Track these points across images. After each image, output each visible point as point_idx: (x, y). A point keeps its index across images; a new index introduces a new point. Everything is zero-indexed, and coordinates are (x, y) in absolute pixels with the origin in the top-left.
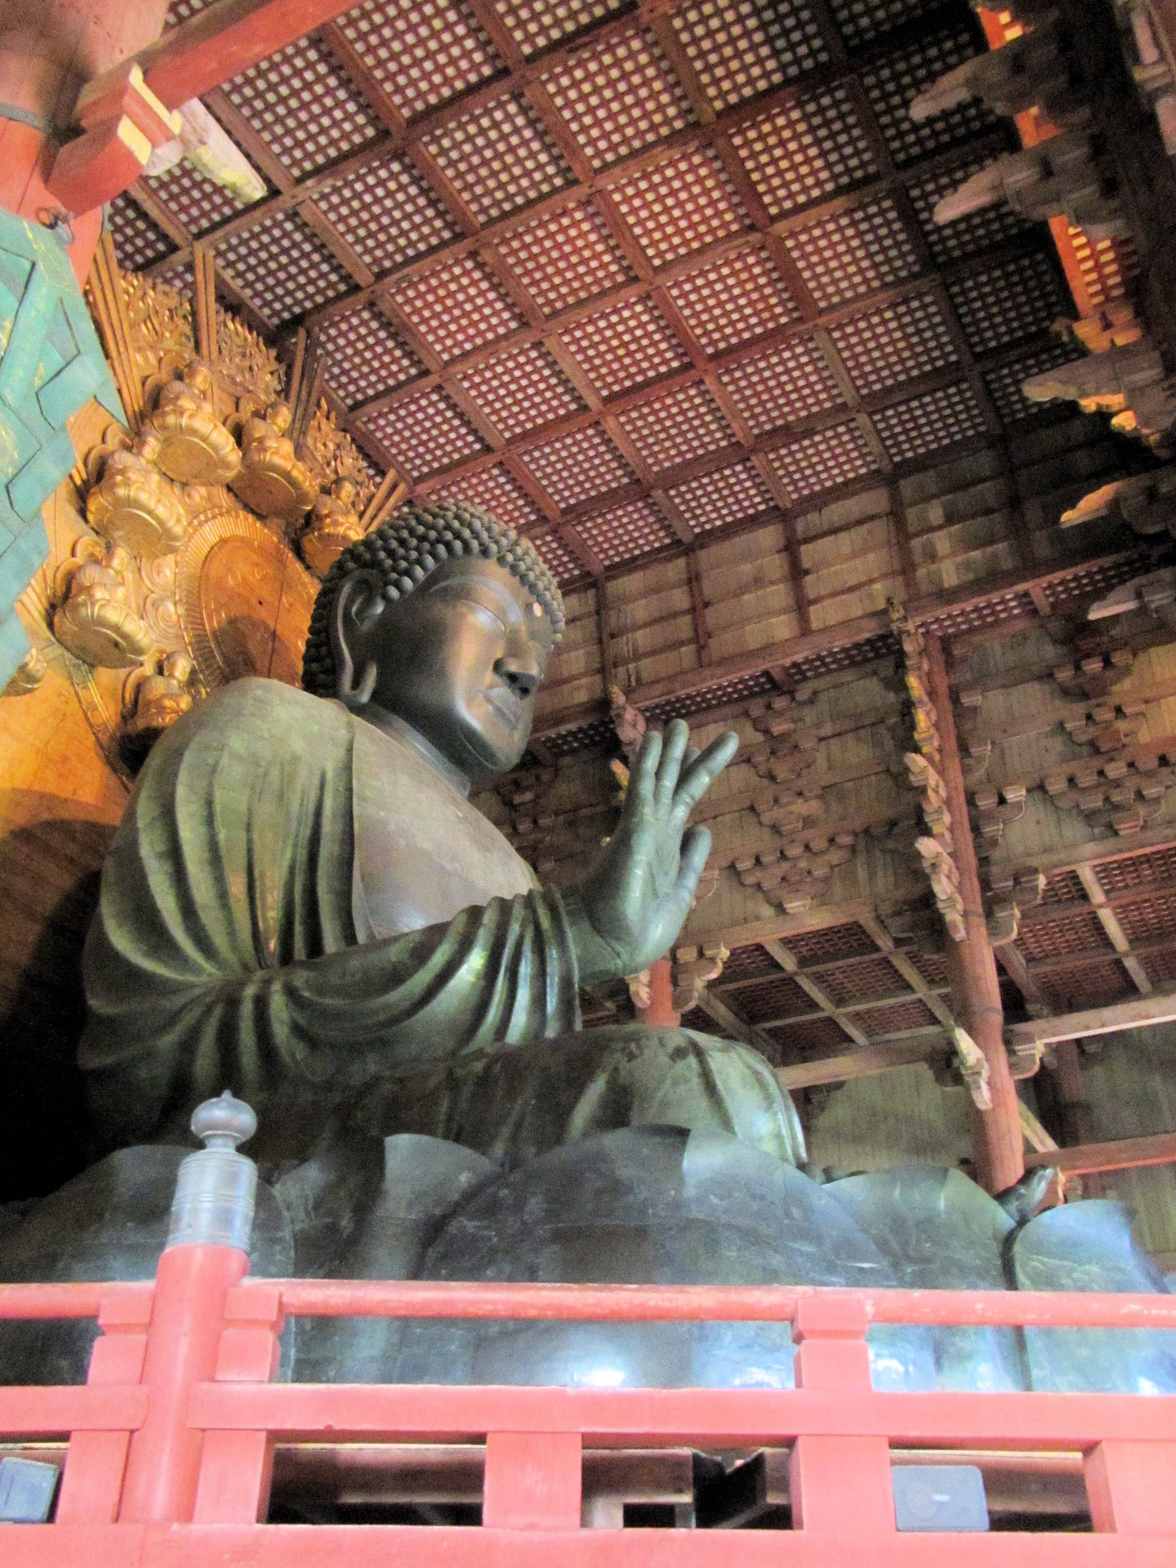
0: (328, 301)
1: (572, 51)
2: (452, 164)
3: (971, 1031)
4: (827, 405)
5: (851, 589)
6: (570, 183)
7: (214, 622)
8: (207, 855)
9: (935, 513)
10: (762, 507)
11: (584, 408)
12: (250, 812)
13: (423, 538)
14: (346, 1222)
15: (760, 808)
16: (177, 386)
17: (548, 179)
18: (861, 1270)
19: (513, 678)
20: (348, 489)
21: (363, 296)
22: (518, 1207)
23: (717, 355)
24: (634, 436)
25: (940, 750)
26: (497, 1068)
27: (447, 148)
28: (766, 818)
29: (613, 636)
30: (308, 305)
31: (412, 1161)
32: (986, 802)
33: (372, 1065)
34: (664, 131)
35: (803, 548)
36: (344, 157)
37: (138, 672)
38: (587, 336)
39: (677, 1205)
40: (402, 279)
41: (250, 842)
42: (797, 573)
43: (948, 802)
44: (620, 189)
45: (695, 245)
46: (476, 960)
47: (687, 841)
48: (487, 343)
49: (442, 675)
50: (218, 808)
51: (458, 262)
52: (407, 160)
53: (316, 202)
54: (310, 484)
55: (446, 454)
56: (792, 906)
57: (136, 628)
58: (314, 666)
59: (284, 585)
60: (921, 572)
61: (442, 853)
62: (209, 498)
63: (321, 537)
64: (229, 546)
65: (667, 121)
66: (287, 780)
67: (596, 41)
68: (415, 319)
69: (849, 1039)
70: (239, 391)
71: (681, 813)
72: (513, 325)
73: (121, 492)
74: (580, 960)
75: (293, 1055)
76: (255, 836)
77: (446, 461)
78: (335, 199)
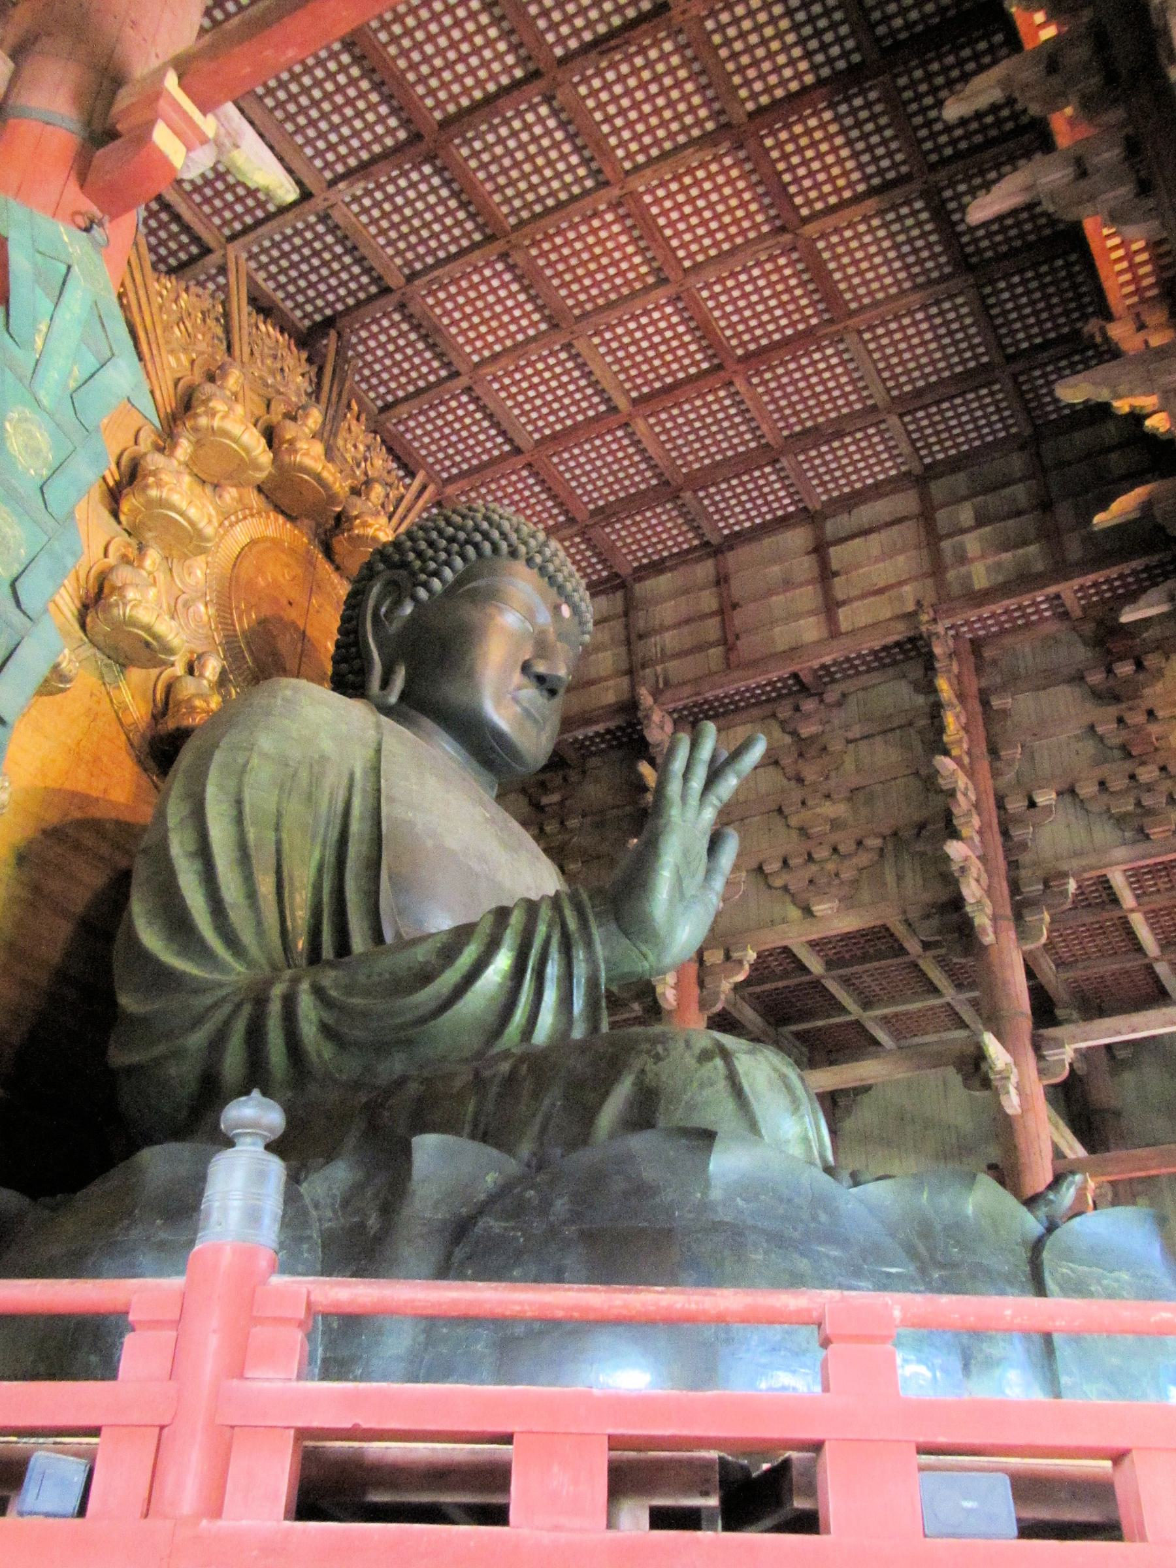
0: (359, 304)
1: (602, 53)
2: (484, 166)
3: (999, 1036)
4: (858, 406)
5: (880, 591)
6: (603, 184)
7: (244, 623)
8: (235, 854)
9: (966, 514)
10: (791, 509)
11: (613, 409)
13: (452, 540)
14: (373, 1222)
15: (786, 811)
16: (209, 388)
17: (578, 180)
18: (889, 1275)
19: (541, 679)
20: (378, 491)
21: (394, 298)
22: (545, 1206)
23: (748, 356)
24: (663, 438)
25: (969, 753)
26: (524, 1068)
27: (475, 150)
28: (794, 821)
29: (641, 637)
30: (340, 307)
31: (440, 1162)
32: (1015, 805)
33: (397, 1064)
34: (696, 132)
35: (832, 550)
36: (375, 160)
37: (168, 673)
38: (617, 338)
39: (705, 1206)
40: (431, 282)
41: (279, 843)
42: (826, 575)
43: (977, 806)
44: (651, 191)
45: (726, 246)
46: (503, 961)
47: (715, 843)
48: (517, 345)
49: (470, 675)
50: (247, 809)
51: (488, 264)
52: (438, 163)
53: (348, 205)
54: (340, 485)
55: (475, 455)
56: (819, 909)
57: (166, 628)
58: (344, 667)
59: (313, 586)
60: (951, 575)
61: (469, 853)
62: (240, 500)
63: (351, 539)
64: (262, 546)
65: (699, 123)
66: (316, 780)
67: (628, 43)
68: (446, 321)
69: (876, 1042)
70: (271, 393)
71: (709, 814)
72: (543, 326)
73: (154, 493)
74: (607, 961)
75: (320, 1056)
76: (284, 836)
77: (475, 462)
78: (367, 202)
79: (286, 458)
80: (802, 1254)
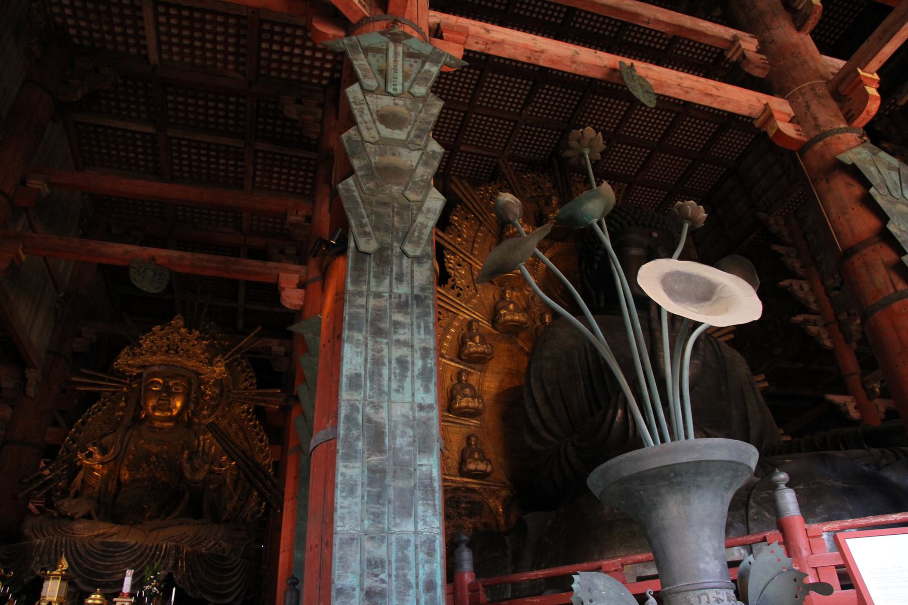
46: (620, 412)
72: (628, 104)
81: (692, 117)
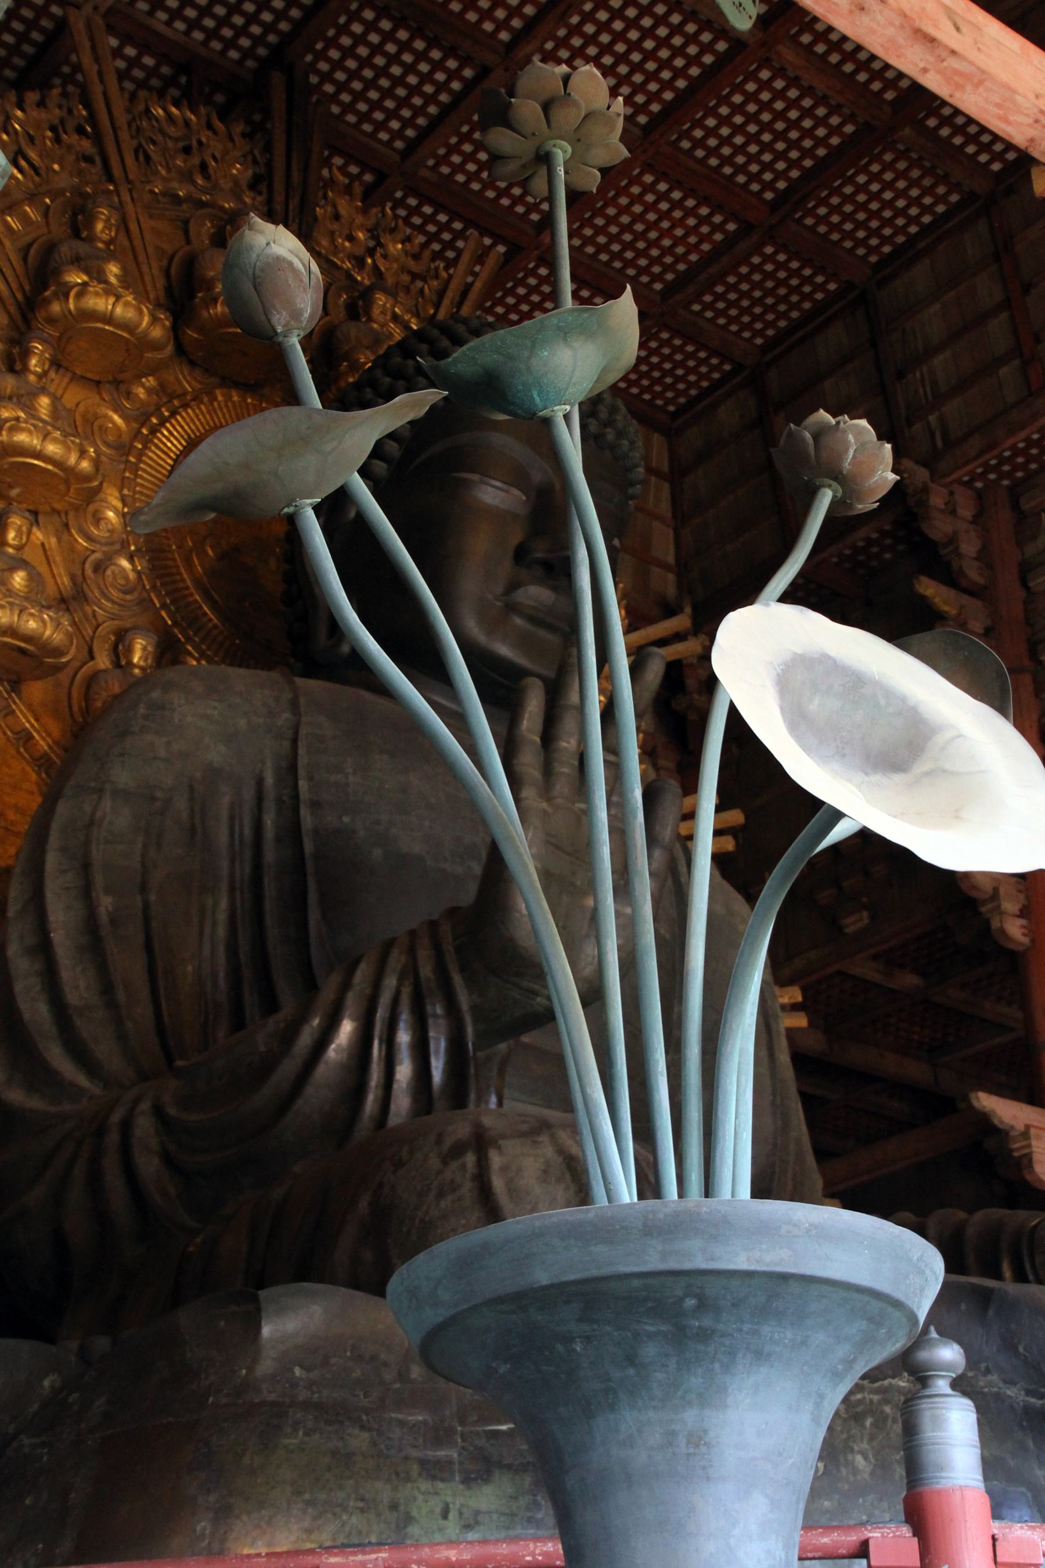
12: (143, 864)
29: (900, 375)
74: (473, 1008)
76: (152, 897)
79: (205, 314)
80: (363, 1428)
81: (779, 72)
